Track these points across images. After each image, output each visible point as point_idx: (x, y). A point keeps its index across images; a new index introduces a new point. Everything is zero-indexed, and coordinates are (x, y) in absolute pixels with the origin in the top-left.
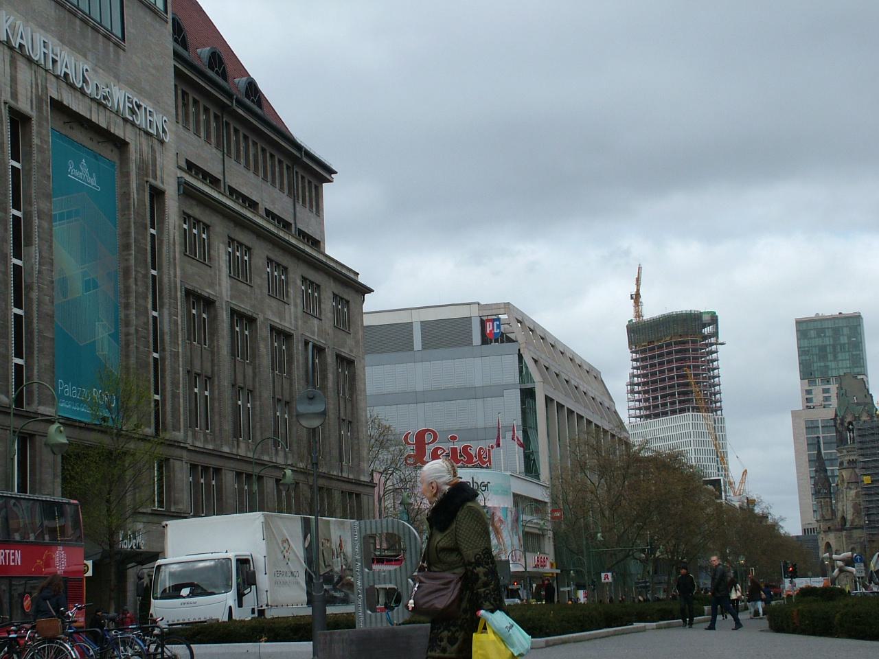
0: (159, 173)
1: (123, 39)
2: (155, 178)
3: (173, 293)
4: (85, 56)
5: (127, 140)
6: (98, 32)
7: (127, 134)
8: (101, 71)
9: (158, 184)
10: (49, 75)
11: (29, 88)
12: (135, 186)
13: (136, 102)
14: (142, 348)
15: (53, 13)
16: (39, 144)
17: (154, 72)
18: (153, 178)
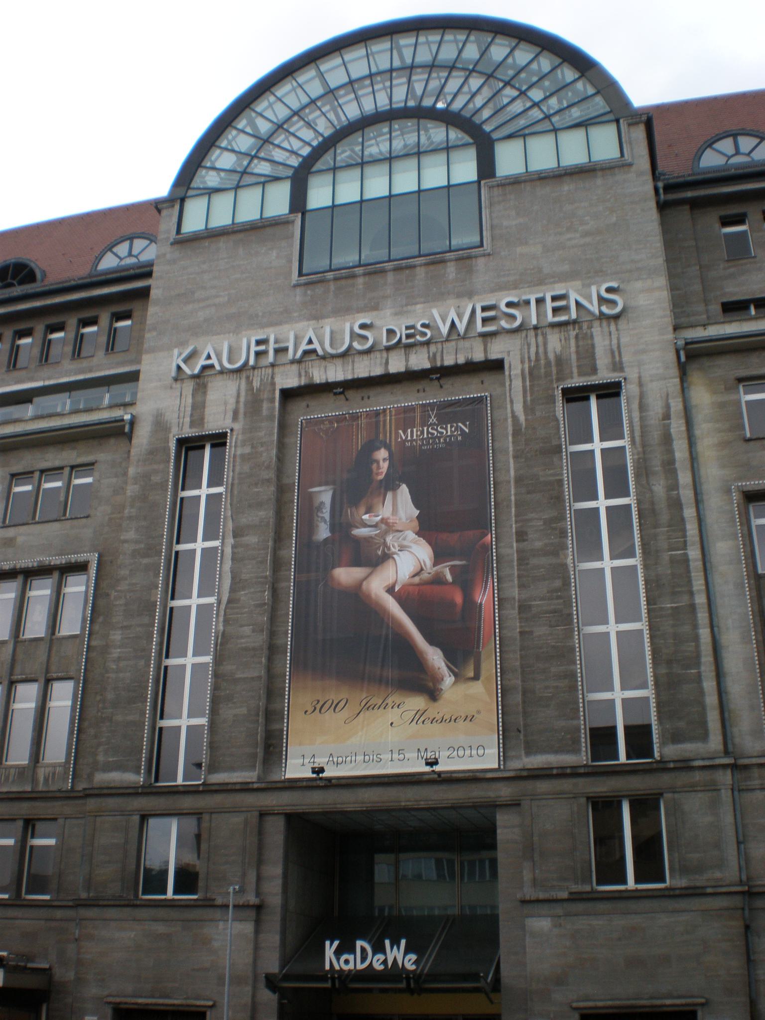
0: (602, 360)
1: (482, 245)
2: (594, 370)
3: (665, 517)
4: (376, 308)
5: (494, 356)
6: (413, 267)
7: (496, 350)
8: (418, 306)
9: (604, 375)
10: (276, 370)
11: (232, 401)
12: (519, 408)
13: (509, 305)
14: (541, 631)
15: (298, 299)
16: (247, 450)
17: (588, 240)
18: (580, 374)
